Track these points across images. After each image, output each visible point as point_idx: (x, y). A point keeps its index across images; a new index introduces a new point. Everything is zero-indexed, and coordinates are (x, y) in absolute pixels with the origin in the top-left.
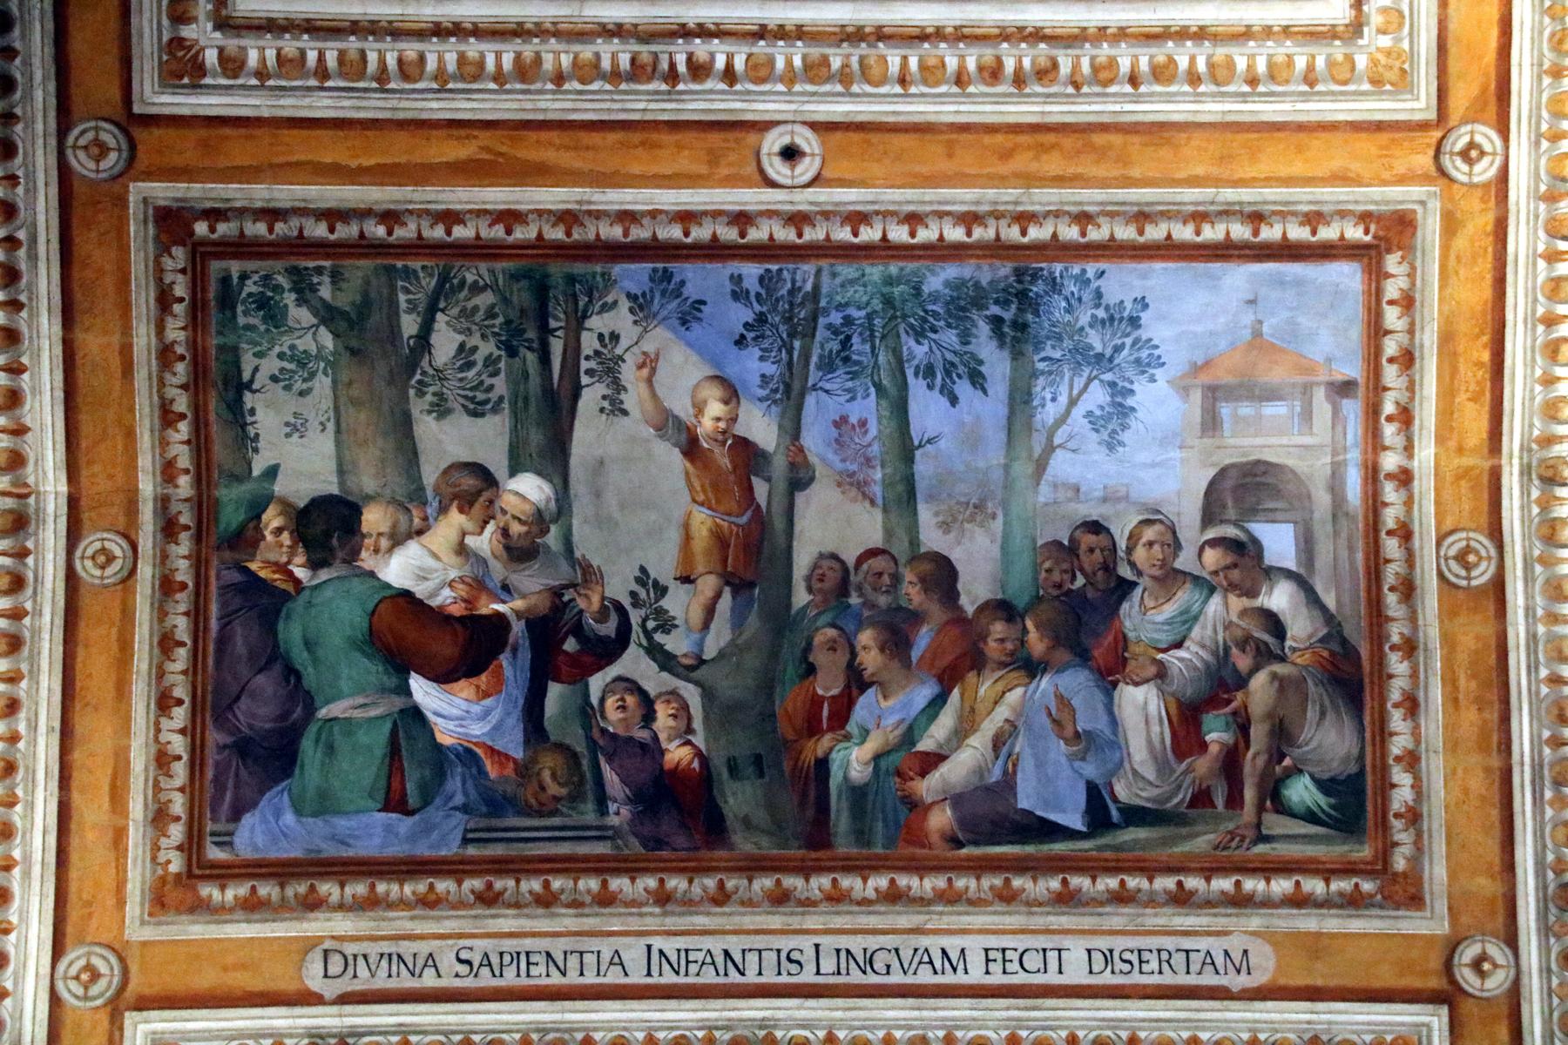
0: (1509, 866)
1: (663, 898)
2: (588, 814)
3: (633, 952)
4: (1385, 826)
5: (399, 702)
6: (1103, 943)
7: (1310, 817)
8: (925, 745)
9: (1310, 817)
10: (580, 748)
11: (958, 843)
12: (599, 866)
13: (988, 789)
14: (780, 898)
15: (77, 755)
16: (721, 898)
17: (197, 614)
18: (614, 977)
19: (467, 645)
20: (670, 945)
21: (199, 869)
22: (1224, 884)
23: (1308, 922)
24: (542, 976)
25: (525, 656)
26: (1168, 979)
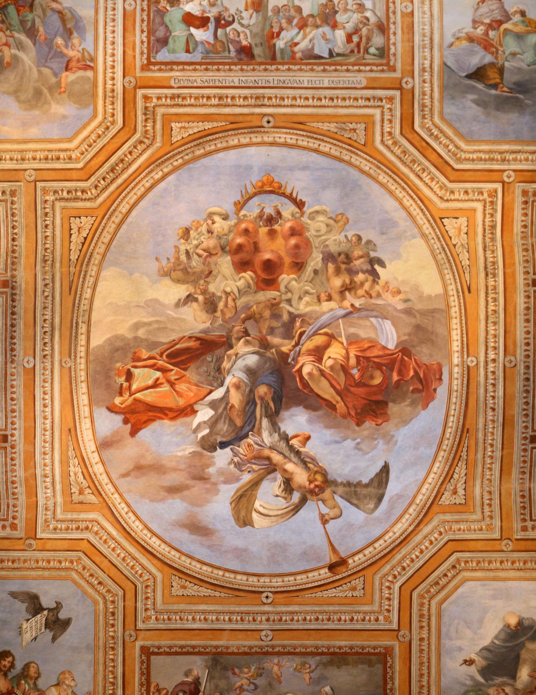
0: (413, 64)
1: (242, 70)
2: (227, 54)
3: (236, 80)
4: (389, 56)
5: (188, 32)
6: (332, 79)
7: (374, 55)
8: (296, 41)
9: (374, 55)
10: (225, 41)
11: (302, 59)
12: (229, 64)
13: (309, 50)
14: (266, 70)
15: (126, 41)
16: (254, 70)
17: (148, 15)
18: (232, 84)
19: (202, 22)
20: (244, 79)
21: (150, 63)
22: (356, 68)
23: (373, 75)
24: (217, 84)
25: (214, 24)
26: (345, 86)
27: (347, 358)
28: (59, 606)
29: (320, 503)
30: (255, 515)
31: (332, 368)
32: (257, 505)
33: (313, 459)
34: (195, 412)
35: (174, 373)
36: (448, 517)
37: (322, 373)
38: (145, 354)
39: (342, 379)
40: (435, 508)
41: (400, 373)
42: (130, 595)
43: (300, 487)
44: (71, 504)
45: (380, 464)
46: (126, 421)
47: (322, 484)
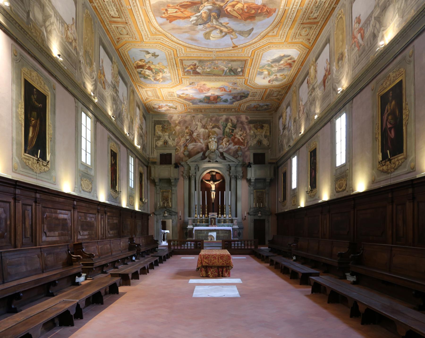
27: (244, 7)
28: (155, 53)
29: (231, 35)
30: (211, 37)
31: (238, 9)
32: (211, 35)
33: (229, 27)
34: (191, 18)
35: (182, 10)
36: (270, 38)
37: (234, 10)
38: (171, 5)
39: (241, 11)
40: (266, 36)
41: (261, 10)
42: (175, 51)
43: (225, 32)
44: (152, 34)
45: (250, 28)
46: (167, 20)
47: (231, 31)
